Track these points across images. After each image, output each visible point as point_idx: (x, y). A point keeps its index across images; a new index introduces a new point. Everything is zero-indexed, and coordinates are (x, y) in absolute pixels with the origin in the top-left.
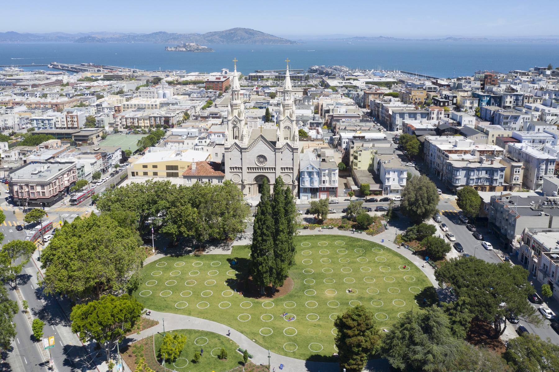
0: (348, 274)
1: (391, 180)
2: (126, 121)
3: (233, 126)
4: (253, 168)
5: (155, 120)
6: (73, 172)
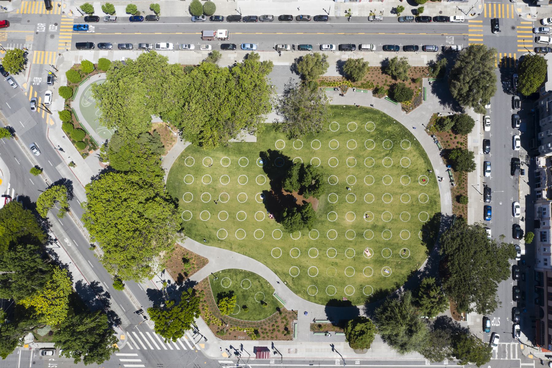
0: (369, 187)
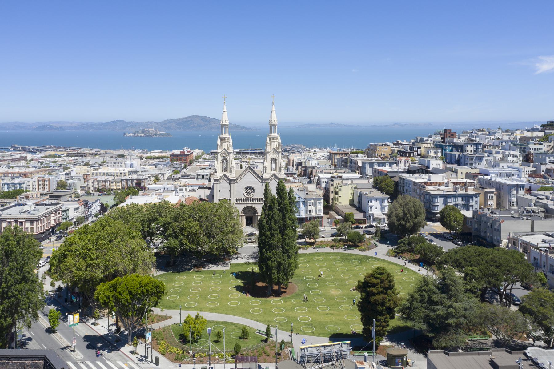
1: (374, 208)
4: (241, 199)
5: (127, 183)
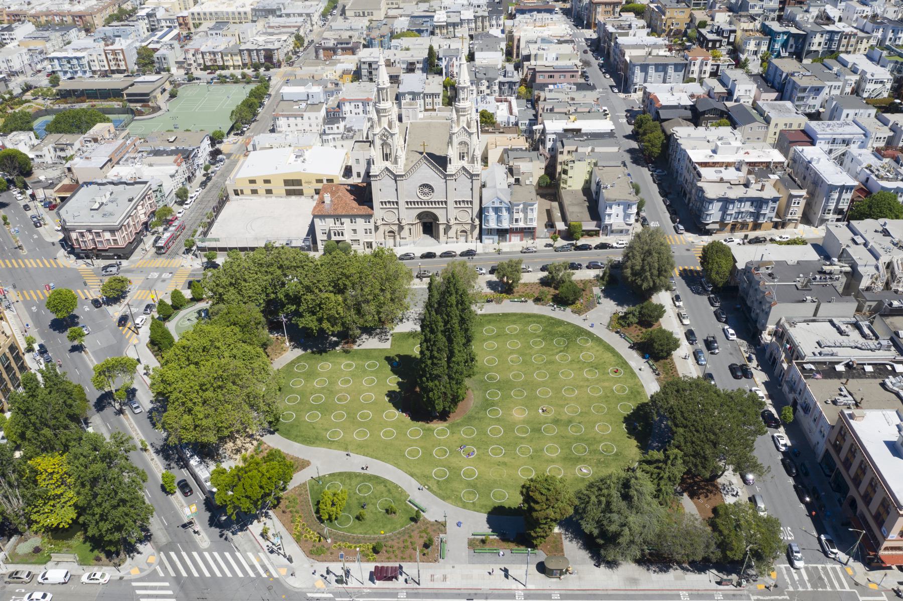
2: (203, 58)
3: (381, 142)
6: (149, 198)
